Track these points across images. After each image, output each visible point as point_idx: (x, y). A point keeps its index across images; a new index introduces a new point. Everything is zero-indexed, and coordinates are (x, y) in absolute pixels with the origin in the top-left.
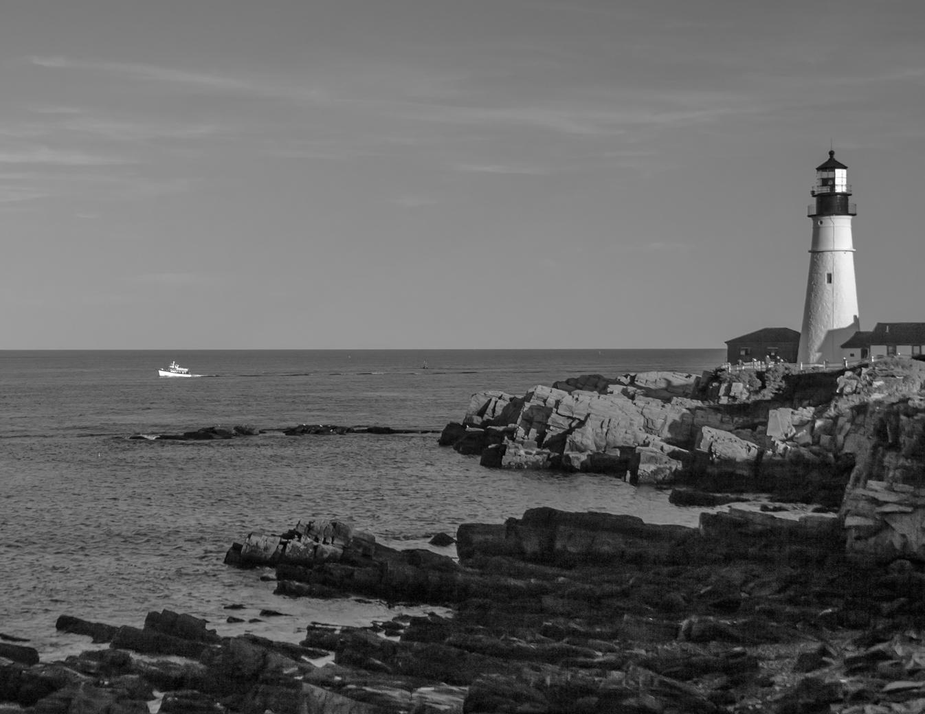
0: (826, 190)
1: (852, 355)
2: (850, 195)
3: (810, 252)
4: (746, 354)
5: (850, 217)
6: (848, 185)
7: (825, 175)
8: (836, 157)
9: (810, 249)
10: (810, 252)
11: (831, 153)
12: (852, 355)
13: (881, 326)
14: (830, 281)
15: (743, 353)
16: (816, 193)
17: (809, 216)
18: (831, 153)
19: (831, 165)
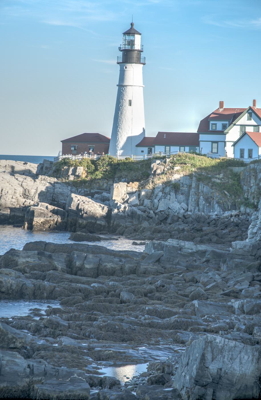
0: (128, 47)
1: (142, 151)
2: (142, 51)
3: (117, 85)
4: (75, 149)
5: (142, 65)
6: (142, 46)
7: (127, 38)
8: (135, 27)
9: (118, 84)
10: (117, 85)
11: (132, 24)
12: (142, 151)
13: (160, 134)
14: (130, 104)
15: (73, 149)
16: (122, 49)
17: (118, 63)
18: (132, 24)
19: (131, 32)
